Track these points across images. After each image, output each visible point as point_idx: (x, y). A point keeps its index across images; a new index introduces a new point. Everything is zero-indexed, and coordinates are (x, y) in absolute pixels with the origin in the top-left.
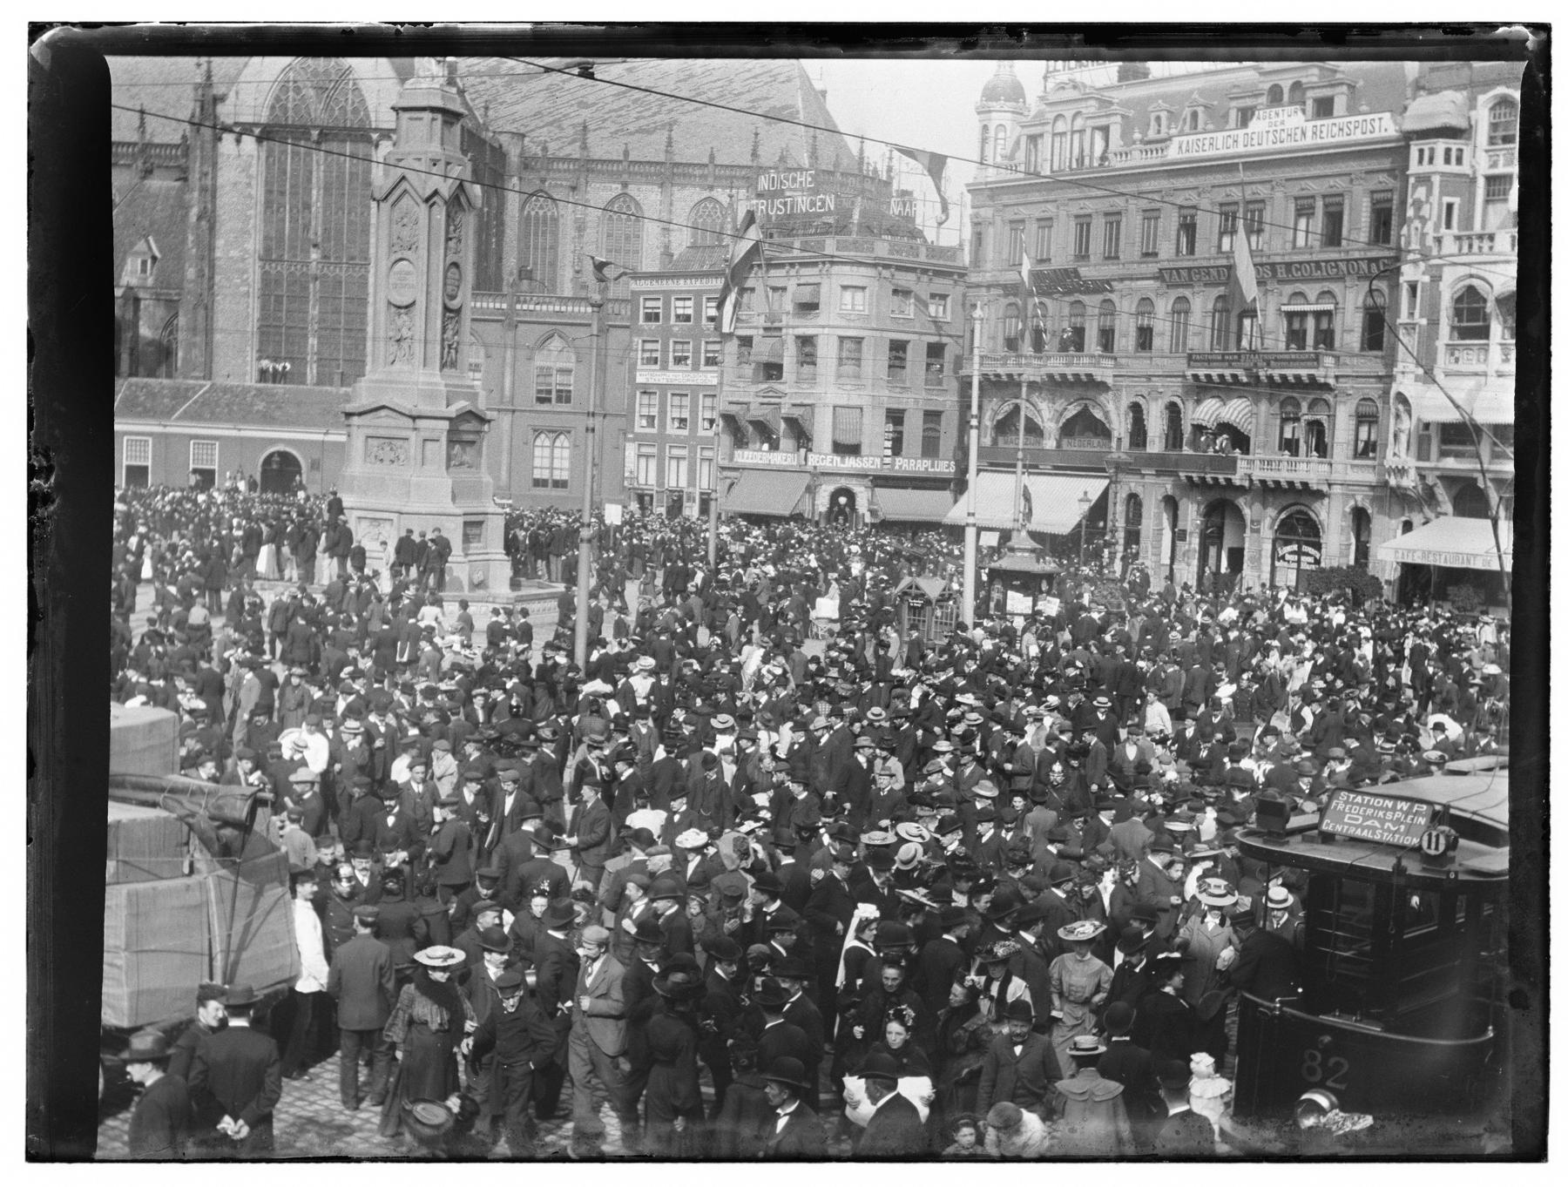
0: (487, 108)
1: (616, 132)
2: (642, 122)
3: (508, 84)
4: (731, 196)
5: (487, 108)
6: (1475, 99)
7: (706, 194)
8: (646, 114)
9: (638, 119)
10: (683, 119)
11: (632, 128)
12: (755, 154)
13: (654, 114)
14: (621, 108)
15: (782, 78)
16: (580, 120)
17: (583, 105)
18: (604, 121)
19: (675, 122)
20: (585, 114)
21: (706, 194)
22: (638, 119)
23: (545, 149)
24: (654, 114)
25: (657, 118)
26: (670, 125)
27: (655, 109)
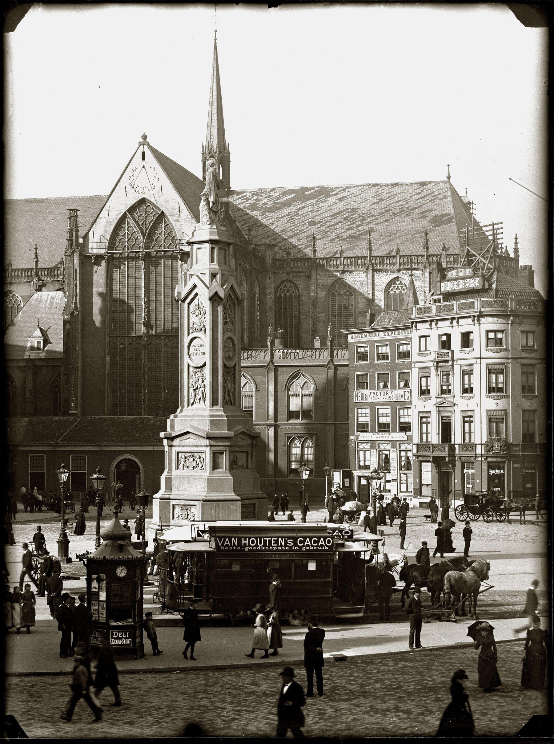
0: (250, 230)
1: (334, 239)
2: (351, 231)
3: (264, 213)
4: (412, 275)
8: (355, 225)
9: (348, 230)
13: (359, 226)
14: (337, 224)
15: (441, 196)
16: (310, 233)
17: (312, 223)
18: (326, 233)
19: (373, 229)
20: (314, 229)
22: (348, 230)
23: (289, 253)
24: (359, 226)
26: (370, 232)
27: (359, 223)
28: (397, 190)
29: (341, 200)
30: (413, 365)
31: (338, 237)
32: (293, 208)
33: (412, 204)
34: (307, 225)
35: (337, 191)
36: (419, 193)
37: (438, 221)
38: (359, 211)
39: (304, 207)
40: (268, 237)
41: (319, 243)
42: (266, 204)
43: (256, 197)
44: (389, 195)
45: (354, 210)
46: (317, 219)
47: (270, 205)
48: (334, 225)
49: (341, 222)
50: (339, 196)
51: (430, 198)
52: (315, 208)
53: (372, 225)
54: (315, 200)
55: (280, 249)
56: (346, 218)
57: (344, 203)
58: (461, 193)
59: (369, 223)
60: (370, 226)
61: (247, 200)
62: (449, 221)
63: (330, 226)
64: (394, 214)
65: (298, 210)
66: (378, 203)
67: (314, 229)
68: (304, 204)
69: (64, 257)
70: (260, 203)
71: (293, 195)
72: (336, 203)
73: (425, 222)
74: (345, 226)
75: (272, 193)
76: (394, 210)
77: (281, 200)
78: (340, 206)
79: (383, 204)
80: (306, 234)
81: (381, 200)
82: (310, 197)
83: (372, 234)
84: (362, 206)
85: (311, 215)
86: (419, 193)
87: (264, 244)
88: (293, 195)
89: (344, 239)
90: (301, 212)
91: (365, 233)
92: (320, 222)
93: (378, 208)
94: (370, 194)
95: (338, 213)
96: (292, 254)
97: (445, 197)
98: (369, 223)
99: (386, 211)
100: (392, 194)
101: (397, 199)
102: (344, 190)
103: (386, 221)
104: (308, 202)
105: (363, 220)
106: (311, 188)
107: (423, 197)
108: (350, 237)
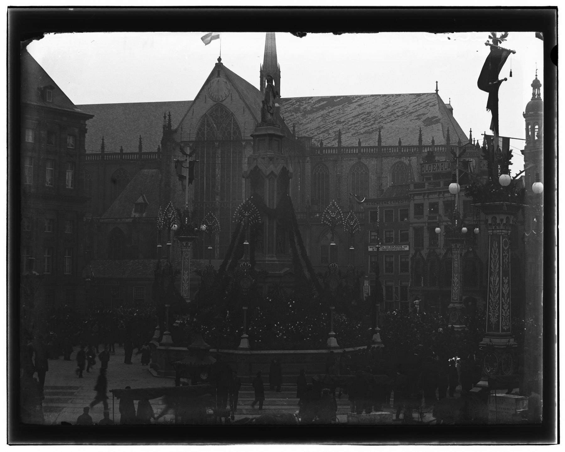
0: (294, 127)
1: (355, 134)
2: (366, 129)
5: (294, 127)
6: (419, 143)
7: (398, 160)
8: (369, 124)
9: (364, 127)
10: (385, 126)
11: (362, 131)
12: (420, 140)
13: (372, 125)
15: (430, 104)
17: (338, 122)
18: (348, 129)
19: (382, 127)
21: (398, 160)
23: (322, 144)
24: (372, 125)
25: (374, 126)
28: (399, 99)
29: (360, 105)
30: (411, 225)
31: (357, 133)
32: (325, 112)
33: (411, 109)
34: (335, 124)
35: (356, 99)
36: (416, 102)
37: (430, 122)
38: (372, 114)
39: (333, 111)
40: (307, 132)
41: (343, 137)
42: (305, 108)
43: (299, 103)
44: (394, 103)
45: (369, 113)
46: (342, 120)
47: (309, 108)
48: (354, 124)
49: (360, 122)
50: (359, 103)
51: (424, 105)
52: (341, 111)
53: (382, 124)
54: (341, 106)
55: (315, 140)
56: (362, 119)
57: (362, 108)
58: (446, 102)
59: (379, 122)
60: (380, 124)
61: (293, 105)
62: (438, 121)
63: (352, 124)
64: (398, 116)
65: (329, 112)
66: (386, 108)
67: (340, 126)
68: (333, 109)
69: (160, 145)
70: (302, 108)
71: (325, 102)
72: (355, 108)
73: (419, 123)
74: (362, 125)
75: (310, 101)
76: (399, 114)
77: (317, 106)
78: (359, 110)
79: (390, 109)
80: (335, 130)
81: (389, 106)
82: (338, 104)
83: (382, 130)
84: (374, 110)
85: (338, 117)
86: (416, 102)
87: (305, 137)
88: (325, 102)
89: (362, 134)
90: (331, 114)
91: (376, 130)
92: (344, 122)
93: (386, 113)
94: (380, 102)
95: (358, 115)
96: (324, 144)
97: (435, 105)
98: (379, 122)
99: (392, 114)
100: (397, 101)
101: (400, 105)
102: (362, 99)
103: (392, 121)
104: (335, 108)
105: (375, 121)
106: (339, 97)
107: (419, 105)
108: (366, 132)
